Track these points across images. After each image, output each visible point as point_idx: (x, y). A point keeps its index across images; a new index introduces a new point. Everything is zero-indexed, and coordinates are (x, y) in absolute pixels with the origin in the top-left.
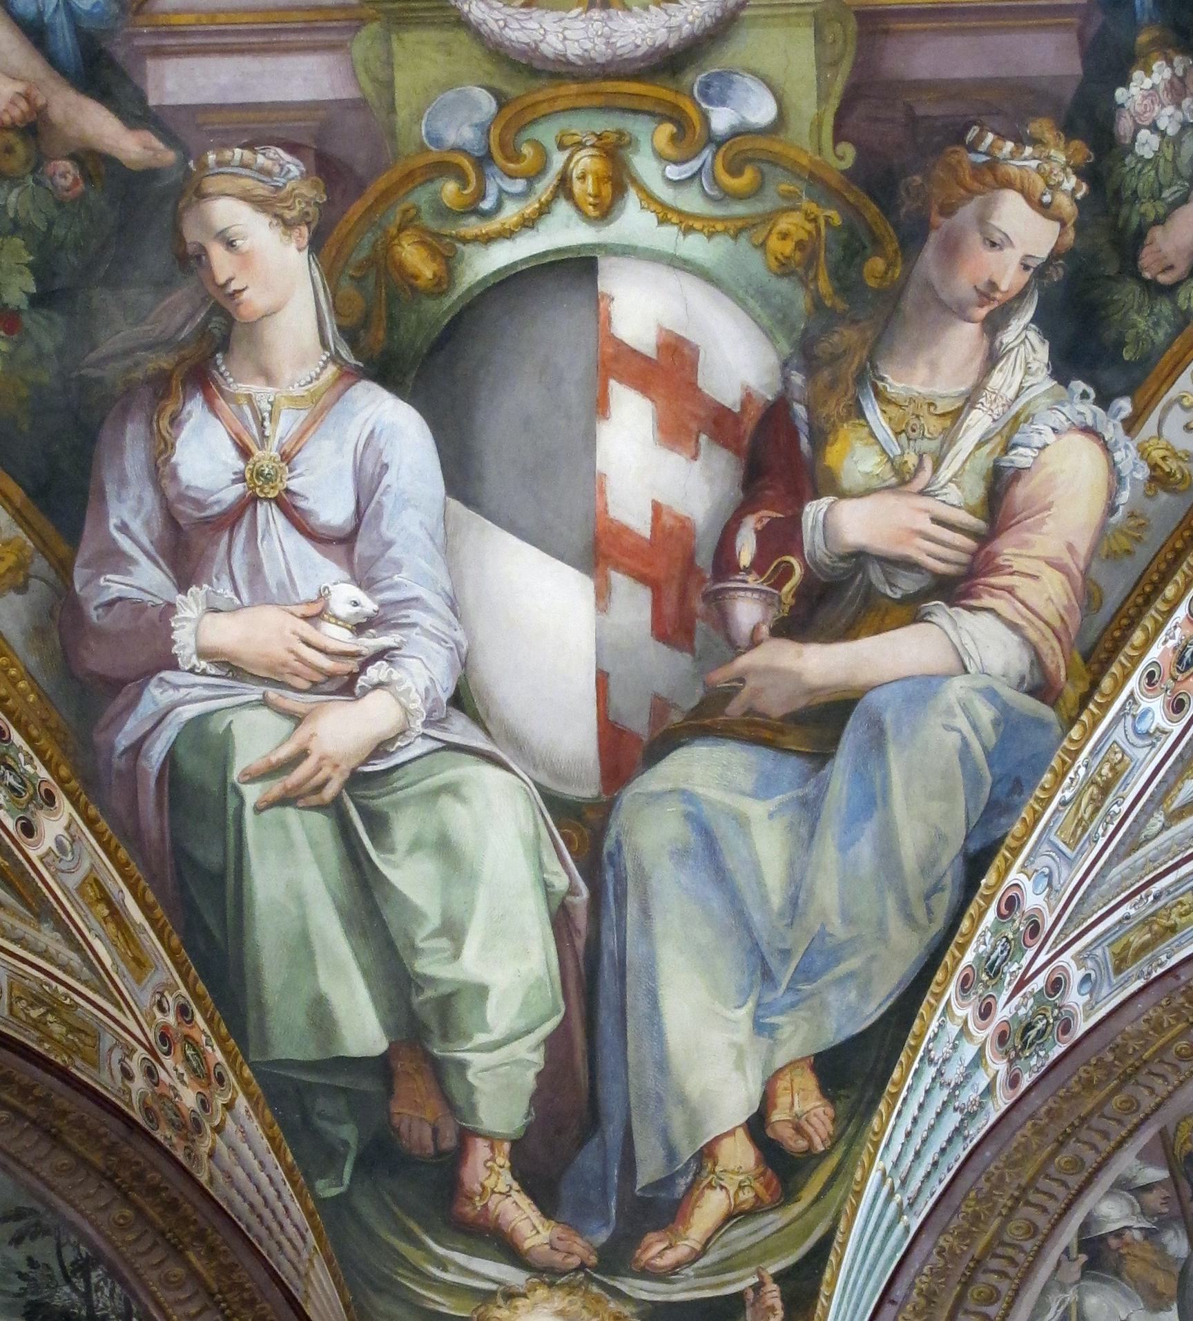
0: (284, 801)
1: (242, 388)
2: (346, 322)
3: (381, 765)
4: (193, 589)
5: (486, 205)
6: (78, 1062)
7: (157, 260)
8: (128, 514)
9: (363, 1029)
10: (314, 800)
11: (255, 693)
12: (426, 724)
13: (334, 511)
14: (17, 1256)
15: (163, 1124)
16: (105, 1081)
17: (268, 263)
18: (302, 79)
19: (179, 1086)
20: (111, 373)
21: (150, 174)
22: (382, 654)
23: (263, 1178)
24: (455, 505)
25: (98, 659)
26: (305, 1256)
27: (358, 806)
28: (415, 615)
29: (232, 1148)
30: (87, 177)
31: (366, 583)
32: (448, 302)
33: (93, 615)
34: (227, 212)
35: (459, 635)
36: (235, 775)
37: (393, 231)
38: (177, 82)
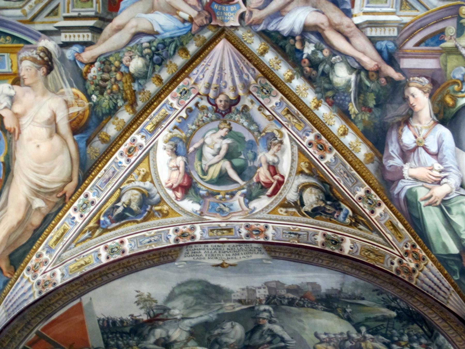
0: (429, 205)
1: (415, 125)
2: (435, 112)
3: (447, 198)
4: (407, 163)
5: (463, 90)
6: (378, 263)
7: (399, 99)
8: (393, 148)
9: (454, 249)
10: (435, 205)
11: (421, 184)
12: (456, 190)
13: (434, 149)
14: (380, 297)
15: (402, 272)
16: (385, 267)
17: (420, 100)
18: (430, 64)
19: (410, 263)
20: (389, 121)
21: (399, 82)
22: (445, 177)
23: (435, 279)
24: (457, 149)
25: (389, 177)
26: (448, 293)
27: (444, 206)
28: (451, 170)
29: (425, 274)
30: (387, 82)
31: (441, 163)
32: (455, 109)
33: (387, 168)
34: (413, 90)
35: (460, 174)
36: (419, 200)
37: (445, 95)
38: (406, 63)
